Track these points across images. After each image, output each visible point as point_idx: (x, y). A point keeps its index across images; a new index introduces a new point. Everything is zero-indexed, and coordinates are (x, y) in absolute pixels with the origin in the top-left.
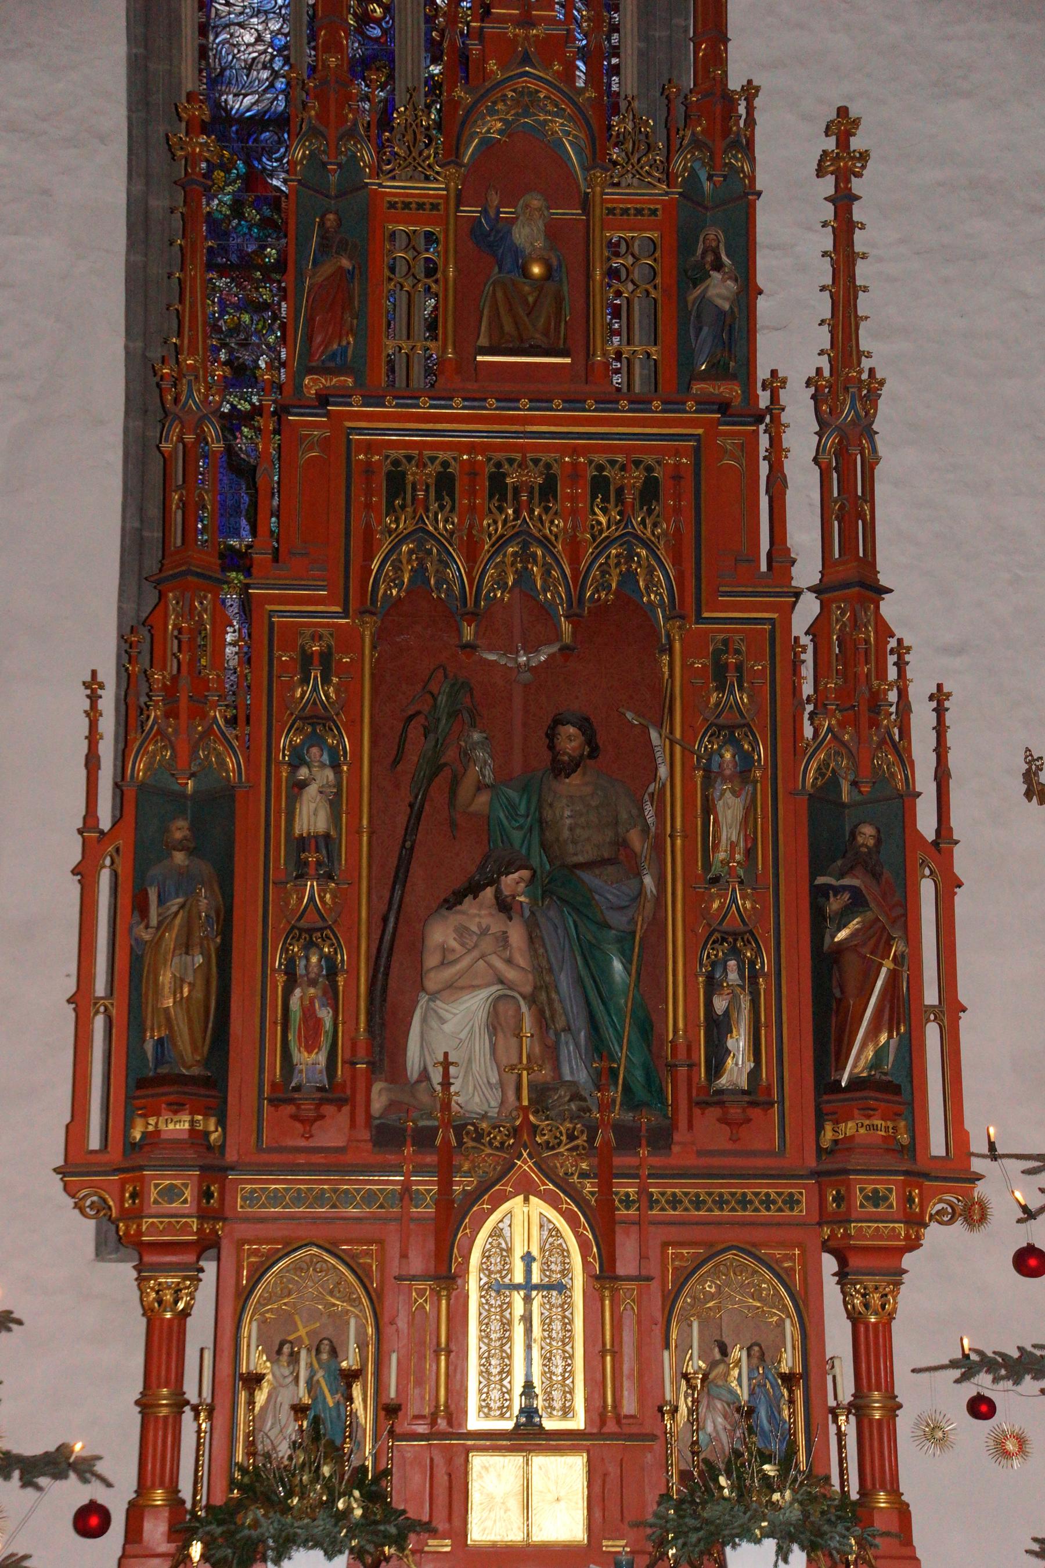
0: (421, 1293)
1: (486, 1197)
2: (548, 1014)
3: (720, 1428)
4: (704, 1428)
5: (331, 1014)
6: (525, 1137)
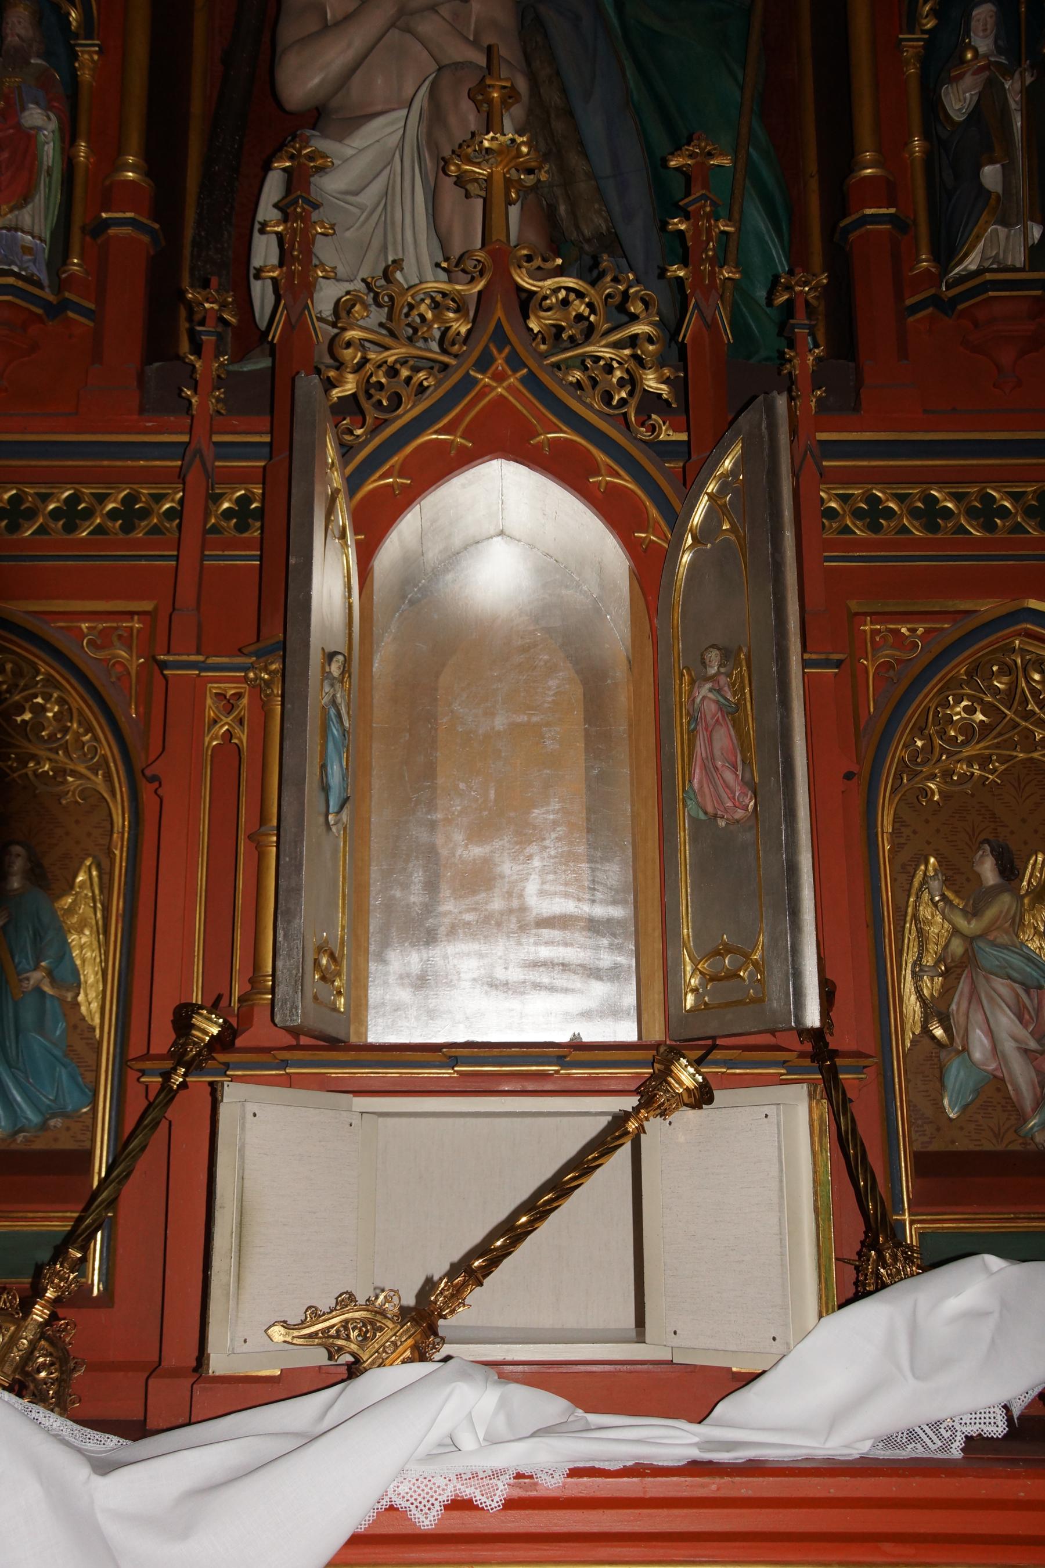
0: (229, 704)
1: (396, 460)
2: (562, 209)
3: (1009, 1046)
4: (965, 1049)
5: (53, 125)
6: (499, 313)
